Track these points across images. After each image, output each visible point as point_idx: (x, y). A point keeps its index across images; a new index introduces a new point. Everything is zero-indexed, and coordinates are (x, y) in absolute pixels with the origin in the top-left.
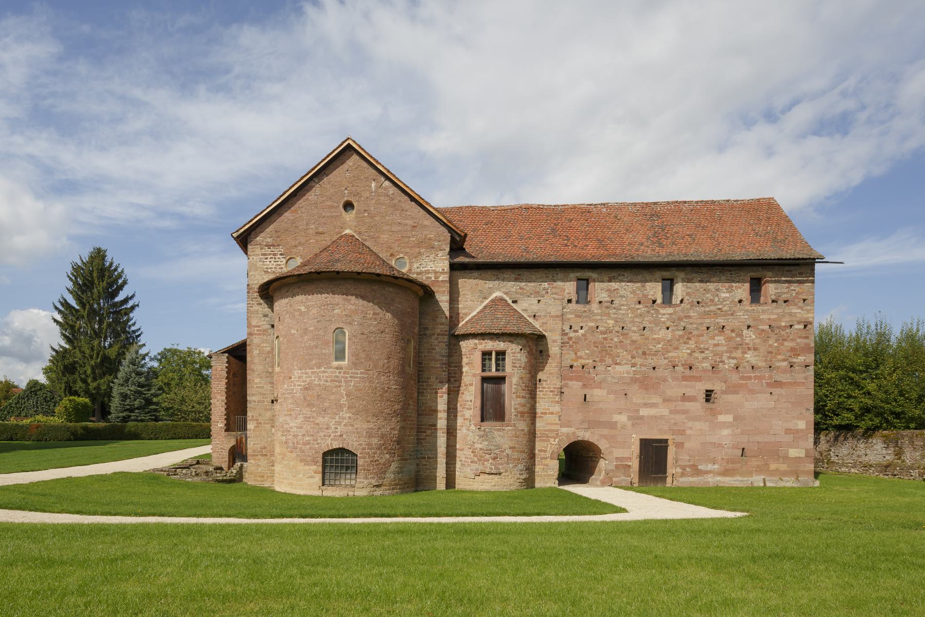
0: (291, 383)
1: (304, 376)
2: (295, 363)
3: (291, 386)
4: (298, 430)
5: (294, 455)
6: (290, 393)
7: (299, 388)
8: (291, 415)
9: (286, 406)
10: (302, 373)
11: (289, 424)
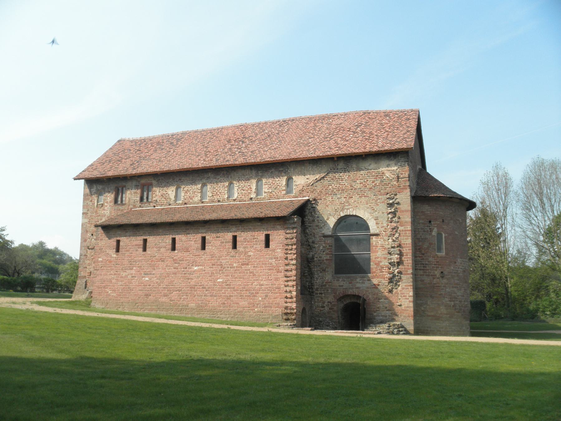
1: (463, 263)
3: (456, 268)
7: (461, 270)
8: (457, 287)
9: (453, 281)
10: (462, 261)
11: (456, 293)
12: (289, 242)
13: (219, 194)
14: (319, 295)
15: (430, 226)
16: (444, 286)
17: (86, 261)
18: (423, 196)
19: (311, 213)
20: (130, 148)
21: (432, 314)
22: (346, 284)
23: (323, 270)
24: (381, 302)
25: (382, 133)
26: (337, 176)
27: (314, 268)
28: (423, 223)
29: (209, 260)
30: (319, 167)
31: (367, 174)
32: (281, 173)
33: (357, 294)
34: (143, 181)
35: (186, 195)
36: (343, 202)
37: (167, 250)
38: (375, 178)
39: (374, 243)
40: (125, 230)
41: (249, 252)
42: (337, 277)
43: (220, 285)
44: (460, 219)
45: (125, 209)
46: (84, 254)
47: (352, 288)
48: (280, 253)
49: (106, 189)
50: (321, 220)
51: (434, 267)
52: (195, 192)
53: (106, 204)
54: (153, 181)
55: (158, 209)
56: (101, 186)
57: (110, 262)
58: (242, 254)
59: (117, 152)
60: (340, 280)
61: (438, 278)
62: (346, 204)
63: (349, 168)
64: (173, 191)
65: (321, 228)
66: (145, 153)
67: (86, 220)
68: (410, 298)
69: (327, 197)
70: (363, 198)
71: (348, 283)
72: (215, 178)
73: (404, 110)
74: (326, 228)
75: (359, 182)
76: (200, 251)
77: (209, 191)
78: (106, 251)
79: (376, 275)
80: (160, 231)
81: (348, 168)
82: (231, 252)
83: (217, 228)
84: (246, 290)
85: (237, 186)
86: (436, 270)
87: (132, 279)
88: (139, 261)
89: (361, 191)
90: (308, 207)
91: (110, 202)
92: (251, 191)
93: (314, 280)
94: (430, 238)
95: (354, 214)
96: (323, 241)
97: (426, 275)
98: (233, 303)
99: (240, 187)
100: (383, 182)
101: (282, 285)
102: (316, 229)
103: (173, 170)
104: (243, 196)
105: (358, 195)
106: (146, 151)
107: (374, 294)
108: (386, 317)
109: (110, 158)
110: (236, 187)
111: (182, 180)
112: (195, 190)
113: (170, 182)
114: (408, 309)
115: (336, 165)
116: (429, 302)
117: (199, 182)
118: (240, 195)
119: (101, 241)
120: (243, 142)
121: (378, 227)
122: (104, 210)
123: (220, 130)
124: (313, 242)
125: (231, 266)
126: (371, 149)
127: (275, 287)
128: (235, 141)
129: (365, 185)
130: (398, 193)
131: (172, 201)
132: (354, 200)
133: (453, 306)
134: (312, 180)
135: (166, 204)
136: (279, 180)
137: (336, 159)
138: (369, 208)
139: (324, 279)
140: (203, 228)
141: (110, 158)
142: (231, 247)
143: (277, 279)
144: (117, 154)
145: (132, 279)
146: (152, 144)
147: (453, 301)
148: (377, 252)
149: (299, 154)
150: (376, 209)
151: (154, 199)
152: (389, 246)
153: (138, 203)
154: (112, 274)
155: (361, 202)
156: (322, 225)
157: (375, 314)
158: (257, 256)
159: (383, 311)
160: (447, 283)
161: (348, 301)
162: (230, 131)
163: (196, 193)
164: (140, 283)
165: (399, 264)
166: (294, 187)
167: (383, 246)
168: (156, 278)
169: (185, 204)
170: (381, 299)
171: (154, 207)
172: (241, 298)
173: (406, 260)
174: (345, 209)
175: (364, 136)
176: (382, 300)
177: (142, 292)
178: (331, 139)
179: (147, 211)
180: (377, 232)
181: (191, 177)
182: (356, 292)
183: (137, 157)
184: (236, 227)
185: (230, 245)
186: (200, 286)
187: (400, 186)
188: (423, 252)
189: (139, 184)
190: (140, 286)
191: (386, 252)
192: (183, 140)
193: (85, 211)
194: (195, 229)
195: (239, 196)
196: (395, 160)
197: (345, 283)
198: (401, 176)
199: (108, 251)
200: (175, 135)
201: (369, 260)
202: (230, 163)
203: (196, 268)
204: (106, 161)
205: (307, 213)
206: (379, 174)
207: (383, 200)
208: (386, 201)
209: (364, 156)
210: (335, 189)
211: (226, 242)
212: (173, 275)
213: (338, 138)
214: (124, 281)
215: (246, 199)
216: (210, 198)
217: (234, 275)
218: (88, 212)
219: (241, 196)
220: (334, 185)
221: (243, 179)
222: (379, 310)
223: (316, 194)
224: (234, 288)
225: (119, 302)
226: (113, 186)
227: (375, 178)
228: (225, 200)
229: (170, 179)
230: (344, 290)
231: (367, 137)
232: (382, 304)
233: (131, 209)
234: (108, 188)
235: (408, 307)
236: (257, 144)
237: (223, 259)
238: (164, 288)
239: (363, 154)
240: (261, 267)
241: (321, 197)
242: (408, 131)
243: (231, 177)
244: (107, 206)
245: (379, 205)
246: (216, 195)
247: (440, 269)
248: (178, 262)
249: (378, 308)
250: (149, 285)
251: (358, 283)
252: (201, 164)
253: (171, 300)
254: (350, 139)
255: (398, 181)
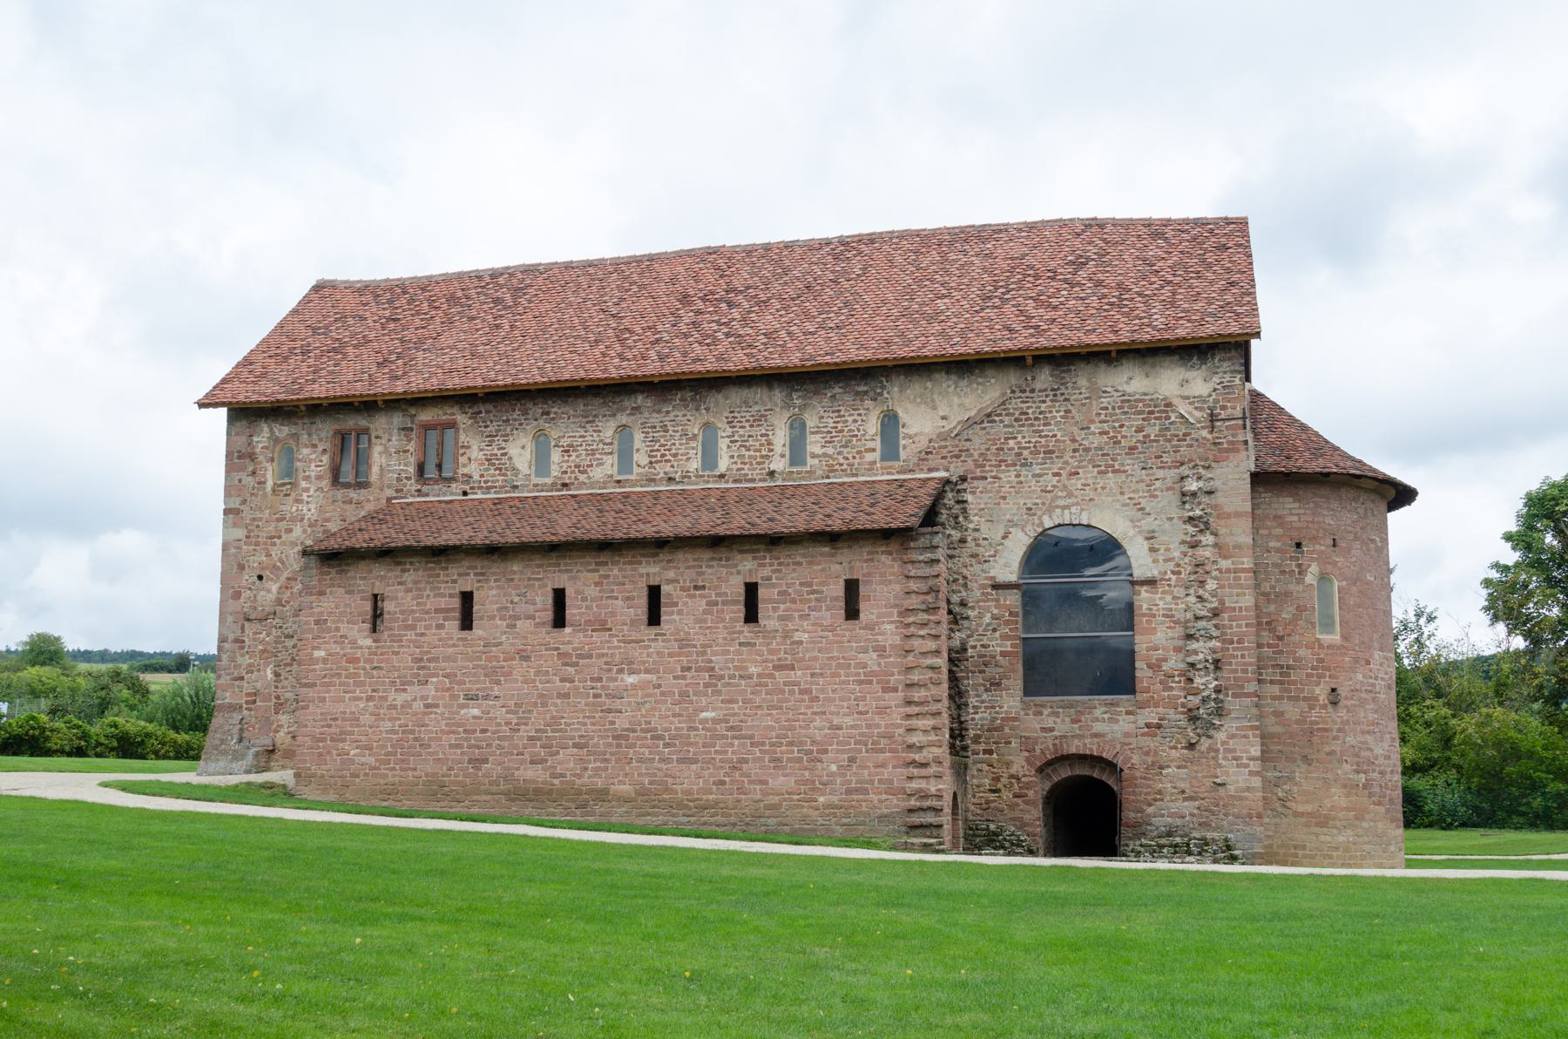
0: (1371, 671)
2: (1375, 635)
3: (1371, 678)
4: (1386, 762)
5: (1381, 809)
6: (1371, 692)
7: (1383, 683)
9: (1363, 715)
11: (1371, 750)
12: (914, 601)
13: (669, 457)
14: (981, 756)
15: (1298, 559)
16: (1339, 730)
17: (239, 660)
18: (1282, 472)
19: (957, 517)
20: (361, 313)
21: (1309, 808)
22: (1062, 725)
23: (991, 684)
24: (1168, 775)
25: (1157, 289)
26: (1030, 411)
27: (968, 678)
28: (1278, 550)
29: (671, 655)
30: (978, 384)
31: (1120, 408)
32: (862, 400)
33: (1095, 754)
34: (427, 415)
35: (568, 461)
36: (1049, 488)
37: (537, 625)
38: (1143, 419)
39: (1145, 606)
40: (399, 563)
41: (798, 630)
42: (1035, 705)
43: (708, 730)
44: (1378, 539)
45: (371, 501)
46: (231, 637)
47: (1081, 737)
48: (890, 633)
49: (304, 438)
50: (984, 539)
51: (1312, 675)
52: (593, 452)
53: (304, 484)
54: (459, 417)
55: (480, 501)
56: (286, 430)
57: (353, 660)
58: (775, 637)
59: (320, 322)
60: (1046, 712)
61: (1324, 707)
62: (1060, 494)
63: (1067, 388)
64: (523, 447)
65: (985, 561)
66: (417, 329)
67: (240, 533)
68: (1252, 763)
69: (1004, 471)
70: (1110, 475)
71: (1068, 720)
72: (659, 412)
73: (1205, 221)
74: (1001, 561)
75: (1097, 431)
76: (642, 627)
77: (638, 450)
78: (338, 629)
79: (1153, 697)
80: (515, 568)
81: (1063, 387)
82: (741, 632)
83: (695, 560)
84: (791, 744)
85: (728, 437)
86: (1318, 684)
87: (425, 714)
88: (447, 659)
89: (1103, 455)
90: (946, 501)
91: (319, 478)
92: (772, 450)
93: (968, 713)
94: (1298, 592)
95: (1085, 523)
96: (992, 600)
97: (1290, 698)
98: (749, 782)
99: (736, 438)
100: (1168, 429)
101: (899, 726)
102: (971, 565)
103: (528, 384)
104: (746, 467)
105: (1094, 467)
106: (418, 322)
107: (1147, 753)
108: (1183, 817)
109: (302, 340)
110: (722, 437)
111: (552, 416)
112: (595, 447)
113: (516, 420)
114: (1246, 794)
115: (1029, 378)
116: (1297, 774)
117: (607, 421)
118: (736, 463)
119: (321, 597)
120: (730, 304)
121: (1155, 561)
122: (298, 501)
123: (648, 263)
124: (963, 604)
125: (742, 673)
126: (1136, 336)
127: (878, 733)
128: (703, 299)
129: (1116, 437)
130: (1213, 464)
131: (520, 476)
132: (1083, 481)
133: (1365, 787)
134: (954, 423)
135: (501, 487)
136: (855, 421)
137: (1030, 361)
138: (1128, 505)
139: (997, 709)
140: (652, 560)
141: (302, 340)
142: (742, 615)
143: (882, 711)
144: (319, 328)
145: (425, 714)
146: (431, 301)
147: (1365, 772)
148: (1153, 631)
149: (918, 344)
150: (1147, 511)
151: (465, 471)
152: (1189, 615)
153: (413, 481)
154: (360, 699)
155: (1103, 488)
156: (987, 554)
157: (1150, 810)
158: (821, 643)
159: (1172, 801)
160: (1348, 721)
161: (1065, 773)
162: (681, 269)
163: (598, 456)
164: (453, 725)
165: (1219, 665)
166: (902, 442)
167: (1172, 616)
168: (504, 709)
169: (565, 485)
170: (1168, 766)
171: (465, 493)
172: (774, 768)
173: (1239, 653)
174: (1057, 507)
175: (1105, 296)
176: (1170, 770)
177: (459, 751)
178: (1004, 301)
179: (443, 505)
180: (1153, 572)
181: (582, 407)
182: (1090, 747)
183: (392, 340)
184: (754, 558)
185: (740, 610)
186: (647, 731)
187: (1219, 443)
188: (1280, 631)
189: (412, 422)
190: (453, 732)
191: (1179, 631)
192: (532, 291)
193: (235, 503)
194: (624, 563)
195: (734, 467)
196: (1203, 367)
197: (1058, 720)
198: (1220, 414)
199: (344, 628)
200: (502, 274)
201: (1131, 655)
202: (709, 367)
203: (631, 679)
204: (291, 350)
205: (945, 516)
206: (1155, 407)
207: (1169, 483)
208: (1177, 486)
209: (1114, 354)
210: (1026, 448)
211: (724, 603)
212: (559, 701)
213: (1025, 299)
214: (400, 719)
215: (756, 474)
216: (640, 470)
217: (750, 699)
218: (242, 507)
219: (739, 466)
220: (1024, 437)
221: (744, 414)
222: (1162, 800)
223: (970, 464)
224: (752, 737)
225: (382, 782)
226: (325, 430)
227: (1143, 419)
228: (690, 477)
229: (514, 410)
230: (1057, 742)
231: (1115, 300)
232: (1171, 782)
233: (389, 500)
234: (310, 435)
235: (1248, 789)
236: (778, 310)
237: (715, 654)
238: (531, 738)
239: (1112, 348)
240: (834, 675)
241: (984, 471)
242: (1232, 284)
243: (707, 409)
244: (307, 490)
245: (1155, 496)
246: (661, 461)
247: (1327, 679)
248: (574, 659)
249: (1160, 792)
250: (484, 731)
251: (1097, 720)
252: (615, 370)
253: (554, 776)
254: (1062, 303)
255: (1213, 427)
